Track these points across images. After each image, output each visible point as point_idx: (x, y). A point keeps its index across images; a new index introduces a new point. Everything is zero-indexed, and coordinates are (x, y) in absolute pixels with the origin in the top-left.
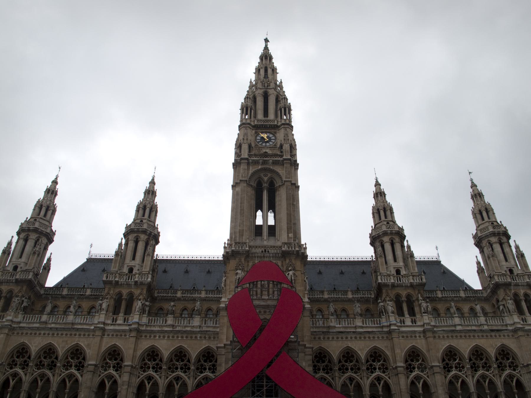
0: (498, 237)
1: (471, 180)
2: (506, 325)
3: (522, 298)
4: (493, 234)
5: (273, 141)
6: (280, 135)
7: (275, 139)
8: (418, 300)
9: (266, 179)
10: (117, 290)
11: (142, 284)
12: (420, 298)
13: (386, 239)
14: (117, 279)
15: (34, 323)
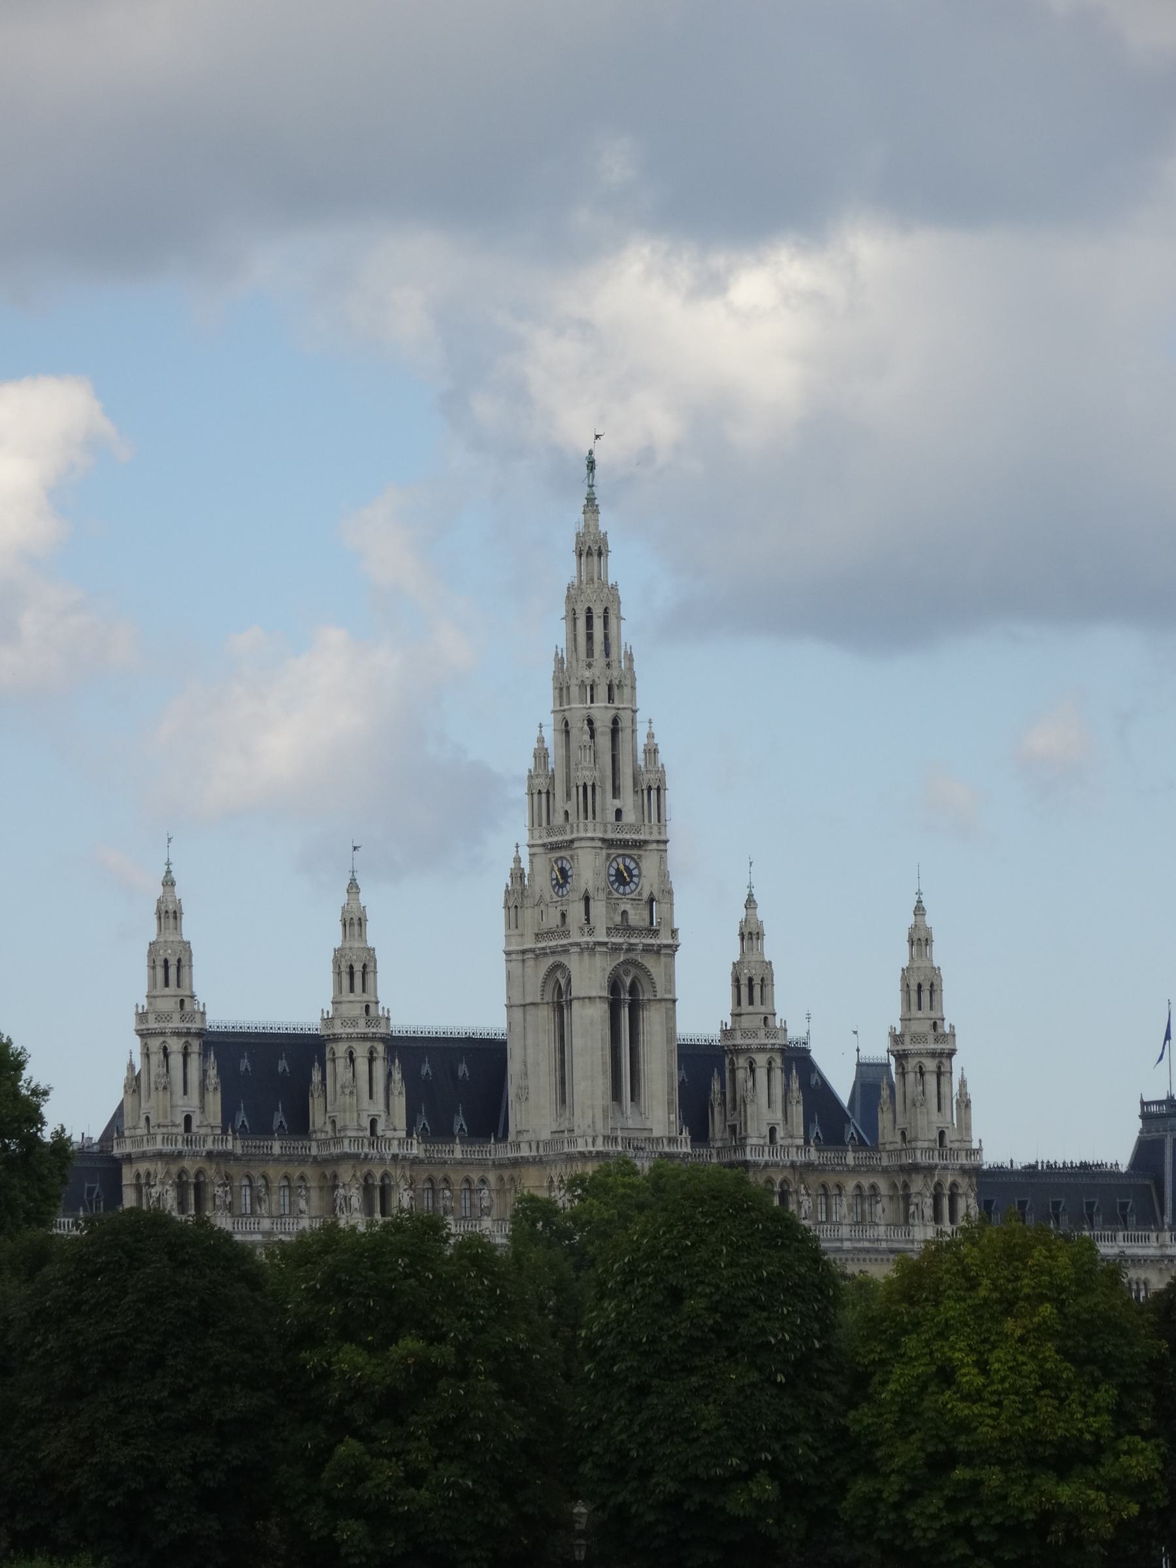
0: (937, 1061)
1: (919, 893)
2: (912, 1242)
3: (947, 1192)
4: (933, 1054)
5: (635, 879)
6: (649, 864)
7: (639, 876)
8: (797, 1192)
9: (628, 981)
10: (365, 1170)
11: (404, 1158)
12: (803, 1192)
13: (761, 1059)
14: (366, 1150)
15: (252, 1233)
